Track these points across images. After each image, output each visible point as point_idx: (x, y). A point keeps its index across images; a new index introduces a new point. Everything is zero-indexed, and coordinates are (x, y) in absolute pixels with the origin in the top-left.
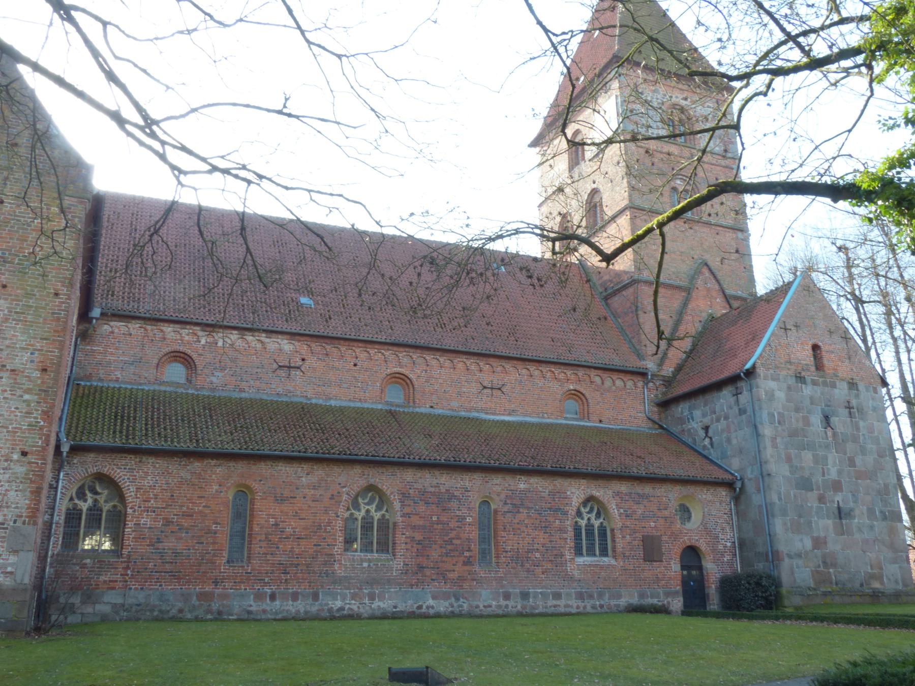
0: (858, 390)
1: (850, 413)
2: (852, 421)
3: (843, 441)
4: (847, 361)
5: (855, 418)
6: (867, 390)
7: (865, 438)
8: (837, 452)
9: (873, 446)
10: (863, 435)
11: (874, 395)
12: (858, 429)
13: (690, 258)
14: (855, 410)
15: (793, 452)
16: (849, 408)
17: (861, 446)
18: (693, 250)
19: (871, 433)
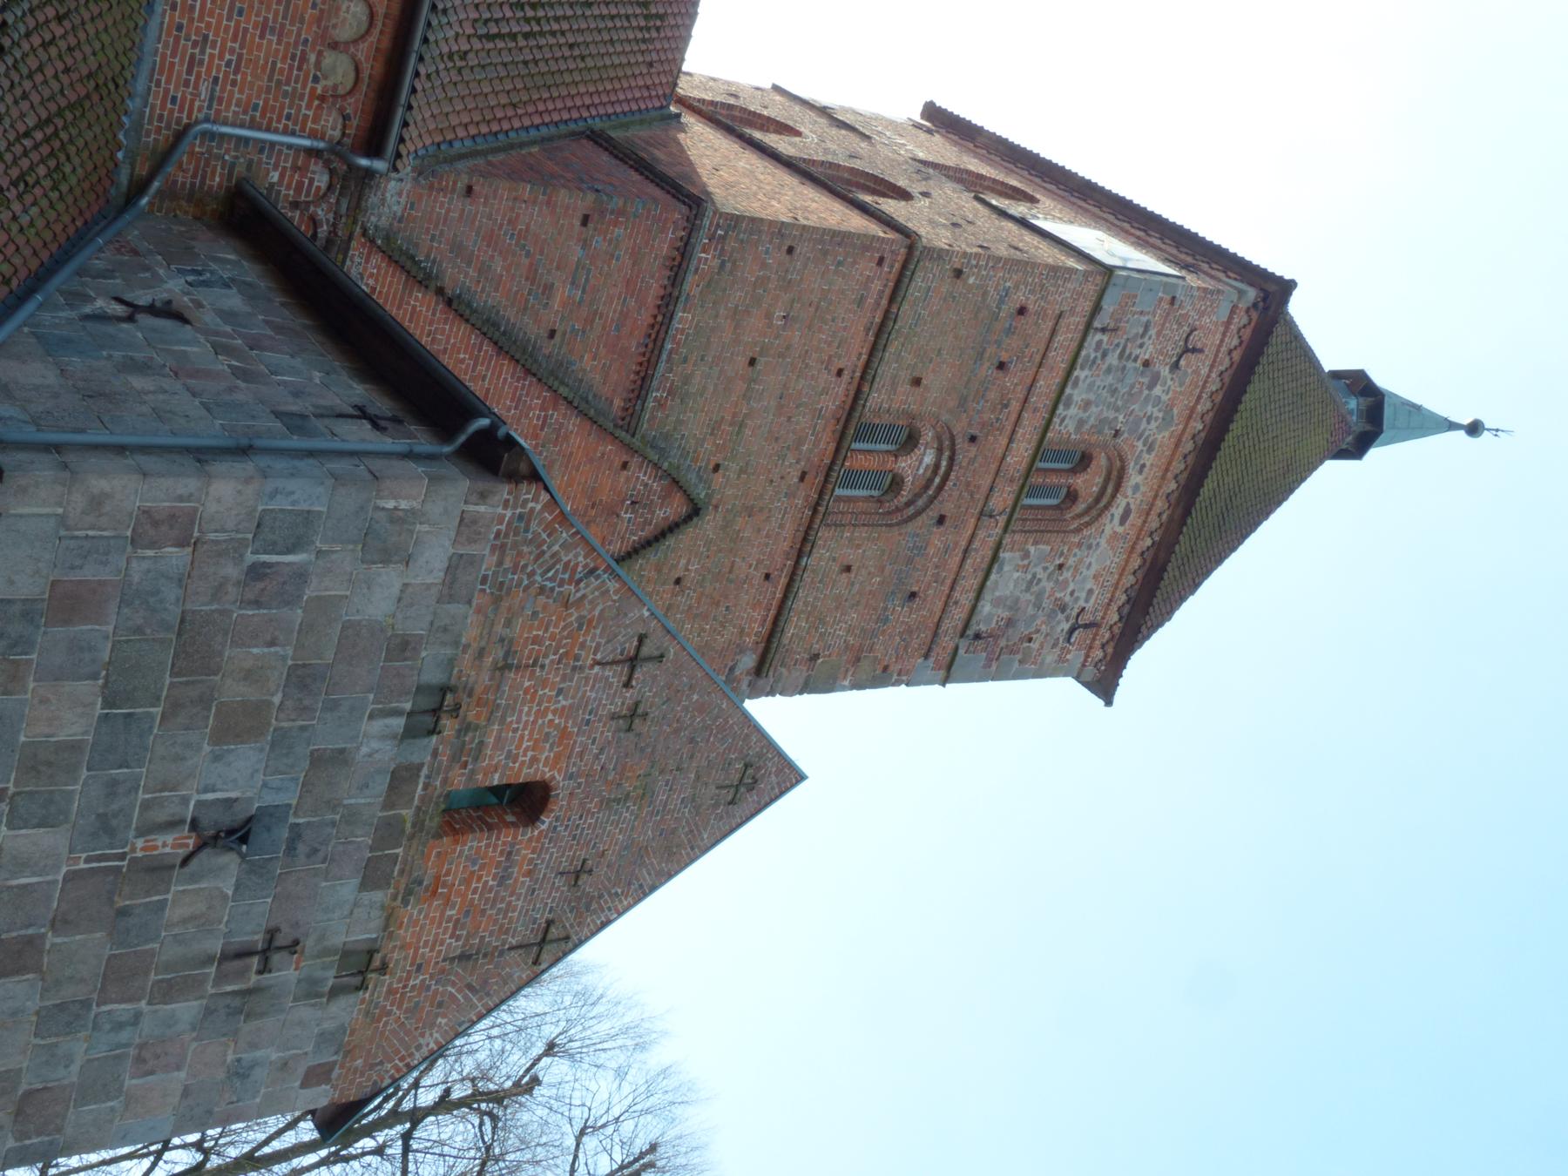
0: (335, 992)
1: (244, 954)
2: (209, 960)
3: (123, 912)
4: (456, 947)
5: (221, 978)
6: (324, 1038)
7: (119, 1026)
8: (71, 877)
9: (75, 1068)
10: (137, 1017)
11: (301, 1071)
12: (167, 992)
13: (714, 460)
14: (254, 979)
15: (100, 633)
16: (270, 949)
17: (86, 1004)
18: (742, 471)
19: (140, 1060)
